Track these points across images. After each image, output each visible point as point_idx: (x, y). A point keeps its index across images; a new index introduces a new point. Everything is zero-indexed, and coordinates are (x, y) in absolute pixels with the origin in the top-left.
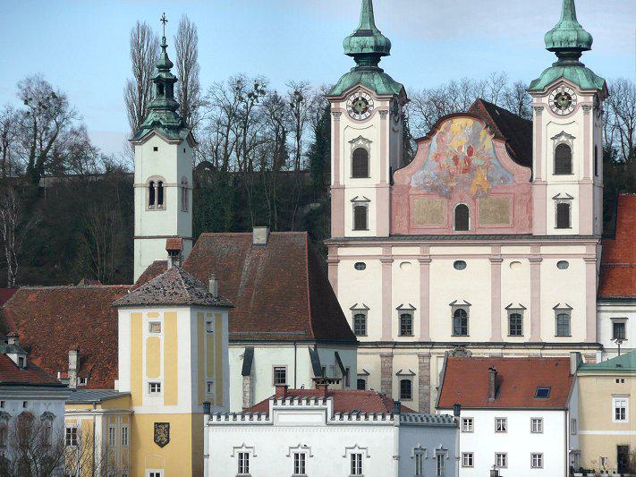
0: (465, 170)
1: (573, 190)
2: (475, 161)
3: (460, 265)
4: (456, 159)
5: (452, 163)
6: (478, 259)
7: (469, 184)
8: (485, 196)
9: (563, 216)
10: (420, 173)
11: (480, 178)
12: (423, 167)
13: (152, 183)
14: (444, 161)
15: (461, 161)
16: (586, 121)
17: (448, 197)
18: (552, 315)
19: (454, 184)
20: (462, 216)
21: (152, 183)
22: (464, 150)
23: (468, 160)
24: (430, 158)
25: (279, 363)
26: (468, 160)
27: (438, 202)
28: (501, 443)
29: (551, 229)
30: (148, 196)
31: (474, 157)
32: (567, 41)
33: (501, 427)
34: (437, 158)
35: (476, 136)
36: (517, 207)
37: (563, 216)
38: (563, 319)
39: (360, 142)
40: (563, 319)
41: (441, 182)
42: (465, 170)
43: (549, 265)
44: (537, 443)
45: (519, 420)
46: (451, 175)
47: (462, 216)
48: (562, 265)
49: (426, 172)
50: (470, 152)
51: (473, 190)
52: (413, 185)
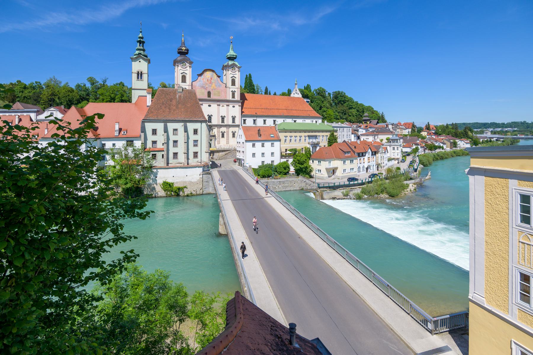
0: (210, 83)
1: (236, 90)
2: (212, 81)
3: (210, 106)
4: (208, 80)
5: (207, 81)
6: (214, 106)
7: (211, 86)
8: (215, 90)
9: (233, 96)
10: (199, 83)
11: (213, 85)
12: (200, 82)
13: (138, 72)
14: (205, 80)
15: (209, 81)
16: (239, 74)
17: (206, 89)
18: (231, 118)
19: (207, 86)
20: (209, 94)
21: (138, 72)
22: (210, 78)
23: (211, 81)
24: (202, 79)
25: (196, 128)
26: (211, 81)
27: (203, 90)
28: (263, 150)
29: (231, 99)
30: (137, 76)
31: (212, 80)
32: (234, 56)
33: (263, 146)
34: (203, 79)
35: (213, 75)
36: (223, 93)
37: (233, 96)
38: (234, 118)
39: (184, 74)
40: (234, 118)
41: (204, 85)
42: (210, 83)
43: (231, 106)
44: (273, 150)
45: (268, 144)
46: (207, 84)
47: (209, 94)
48: (234, 107)
49: (200, 83)
50: (211, 79)
51: (212, 88)
52: (197, 86)
